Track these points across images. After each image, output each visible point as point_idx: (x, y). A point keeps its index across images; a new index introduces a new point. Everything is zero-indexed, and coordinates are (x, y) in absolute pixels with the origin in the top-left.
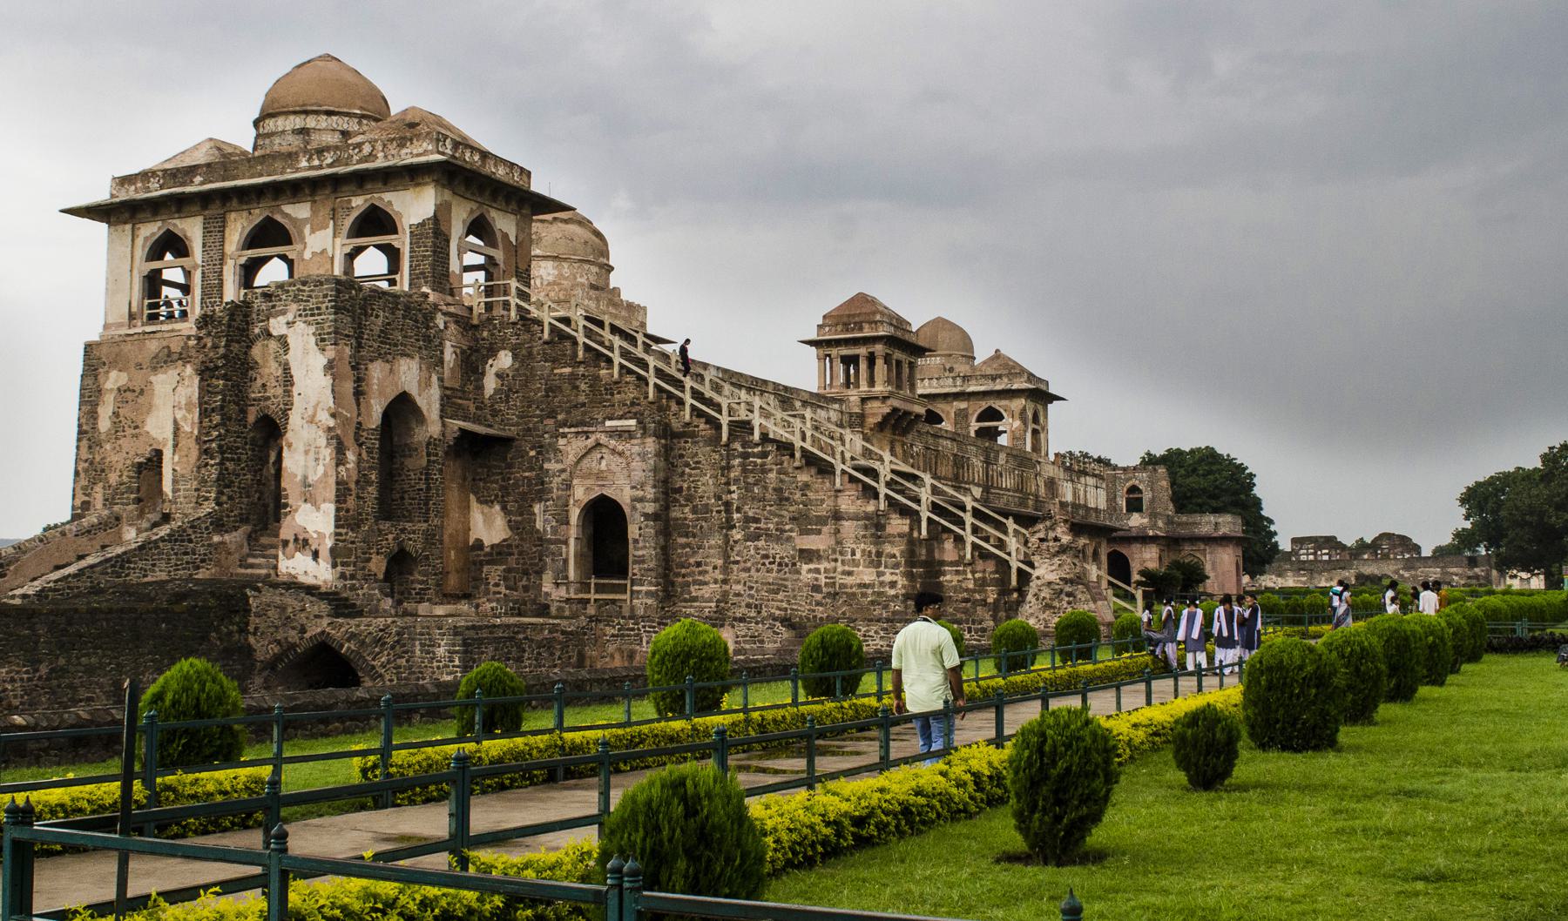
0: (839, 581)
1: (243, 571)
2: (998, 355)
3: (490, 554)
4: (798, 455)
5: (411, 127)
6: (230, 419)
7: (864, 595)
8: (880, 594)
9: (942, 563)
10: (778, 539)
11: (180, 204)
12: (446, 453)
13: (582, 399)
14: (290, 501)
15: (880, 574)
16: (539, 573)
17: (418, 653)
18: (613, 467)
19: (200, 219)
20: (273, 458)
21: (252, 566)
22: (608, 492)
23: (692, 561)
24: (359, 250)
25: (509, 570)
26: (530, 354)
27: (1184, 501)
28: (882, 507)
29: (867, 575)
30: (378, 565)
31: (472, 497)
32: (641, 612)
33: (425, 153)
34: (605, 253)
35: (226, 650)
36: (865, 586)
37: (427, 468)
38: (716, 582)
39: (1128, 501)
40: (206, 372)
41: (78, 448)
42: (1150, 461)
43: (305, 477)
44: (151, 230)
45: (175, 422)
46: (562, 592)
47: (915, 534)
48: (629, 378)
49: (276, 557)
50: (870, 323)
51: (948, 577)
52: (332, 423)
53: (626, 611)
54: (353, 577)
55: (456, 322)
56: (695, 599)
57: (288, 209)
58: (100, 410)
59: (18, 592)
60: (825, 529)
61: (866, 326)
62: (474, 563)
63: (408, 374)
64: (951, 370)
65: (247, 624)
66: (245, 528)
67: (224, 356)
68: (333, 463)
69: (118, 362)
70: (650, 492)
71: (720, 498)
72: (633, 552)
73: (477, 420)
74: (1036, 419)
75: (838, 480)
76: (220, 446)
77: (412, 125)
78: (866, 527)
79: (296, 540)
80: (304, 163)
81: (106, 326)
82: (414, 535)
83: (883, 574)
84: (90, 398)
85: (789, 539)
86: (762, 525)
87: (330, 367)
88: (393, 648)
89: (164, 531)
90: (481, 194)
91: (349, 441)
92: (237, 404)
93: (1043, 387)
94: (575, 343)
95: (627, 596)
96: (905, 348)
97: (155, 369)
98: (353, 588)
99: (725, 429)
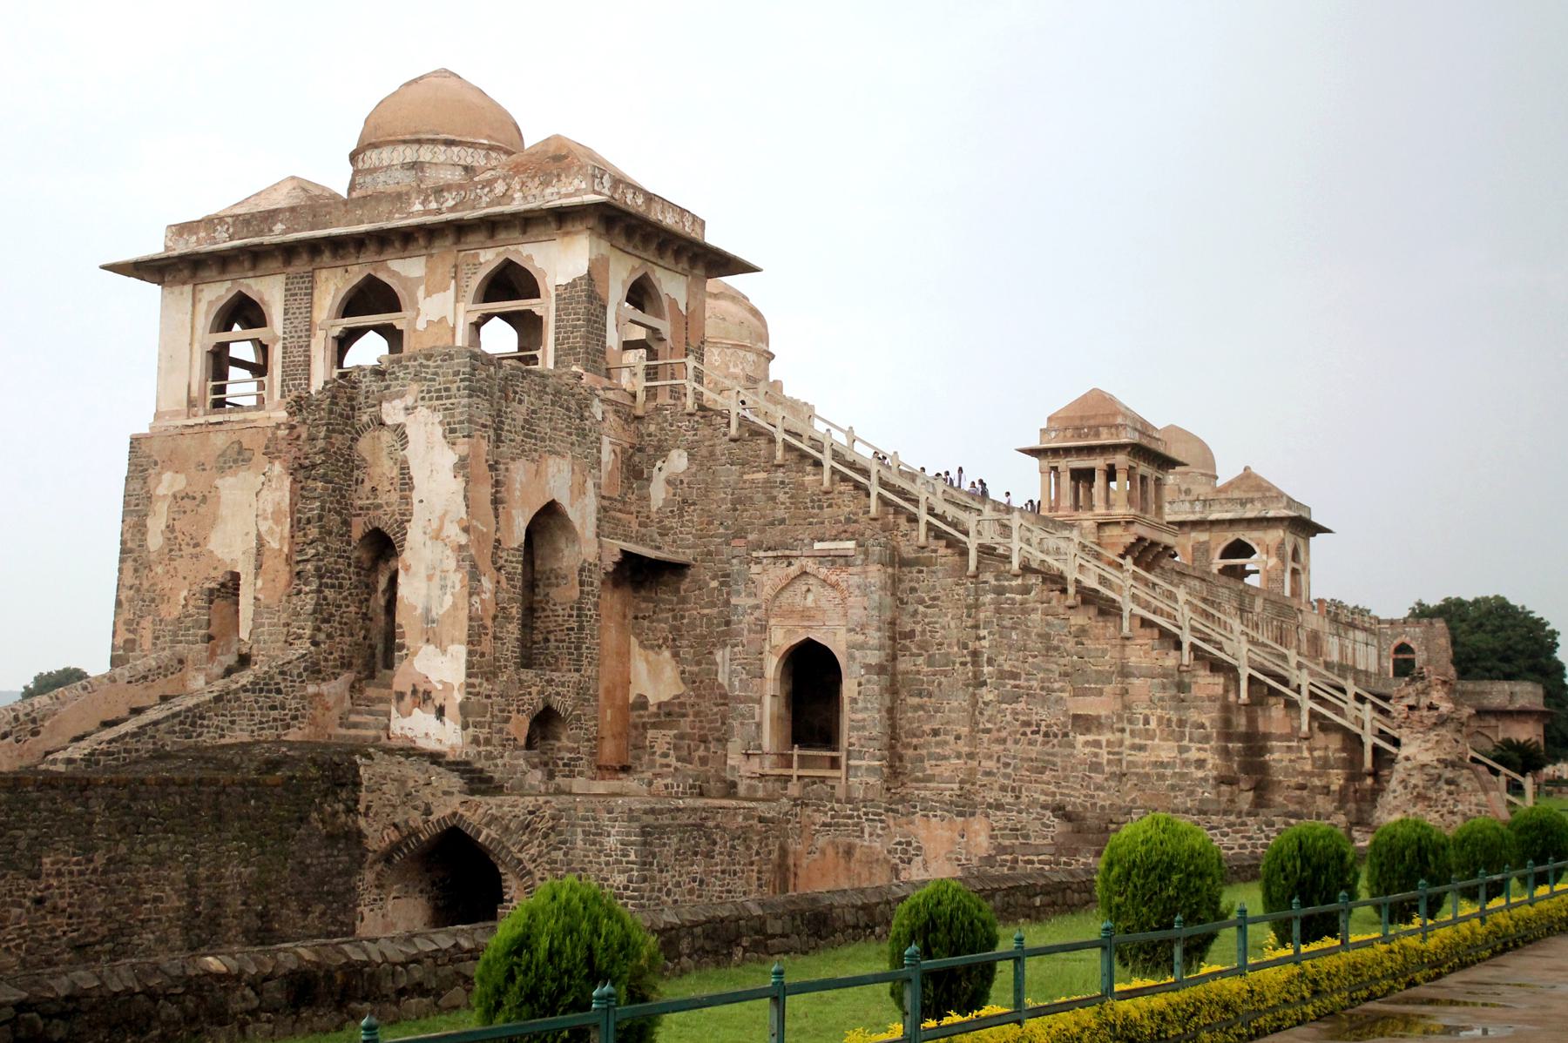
0: (1126, 758)
1: (343, 731)
2: (1247, 475)
3: (658, 715)
4: (1071, 590)
5: (559, 158)
6: (330, 533)
7: (1161, 777)
8: (1183, 776)
9: (1267, 736)
10: (1044, 700)
11: (255, 257)
12: (603, 583)
13: (781, 513)
14: (407, 641)
15: (1182, 750)
16: (723, 741)
17: (580, 843)
18: (823, 603)
19: (281, 278)
20: (383, 582)
21: (355, 726)
22: (817, 636)
23: (927, 728)
24: (487, 318)
25: (681, 737)
26: (712, 454)
27: (1468, 664)
28: (1186, 661)
29: (1165, 751)
30: (519, 726)
31: (633, 639)
32: (860, 794)
33: (577, 192)
34: (764, 338)
35: (330, 836)
36: (1162, 765)
37: (580, 602)
38: (959, 756)
39: (1396, 663)
40: (300, 471)
41: (120, 570)
42: (1422, 613)
43: (428, 610)
44: (217, 293)
45: (259, 537)
46: (754, 765)
47: (1232, 697)
48: (843, 487)
49: (388, 714)
50: (1110, 427)
51: (1276, 756)
52: (463, 539)
53: (840, 792)
54: (488, 742)
55: (617, 412)
56: (930, 778)
57: (396, 265)
58: (149, 522)
59: (61, 755)
60: (1108, 688)
61: (1104, 431)
62: (635, 727)
63: (557, 479)
64: (1188, 492)
65: (357, 802)
66: (347, 677)
67: (323, 451)
68: (466, 591)
69: (174, 461)
70: (874, 637)
71: (965, 646)
72: (847, 716)
73: (641, 540)
74: (1295, 556)
75: (1126, 624)
76: (318, 569)
77: (558, 158)
78: (1164, 687)
79: (415, 692)
80: (418, 207)
81: (158, 415)
83: (1187, 749)
84: (136, 507)
85: (1059, 701)
86: (1022, 683)
87: (462, 466)
88: (546, 836)
89: (245, 677)
90: (645, 247)
91: (485, 564)
92: (339, 513)
93: (1305, 515)
94: (772, 441)
95: (841, 773)
96: (1152, 457)
97: (221, 470)
98: (489, 756)
99: (973, 555)
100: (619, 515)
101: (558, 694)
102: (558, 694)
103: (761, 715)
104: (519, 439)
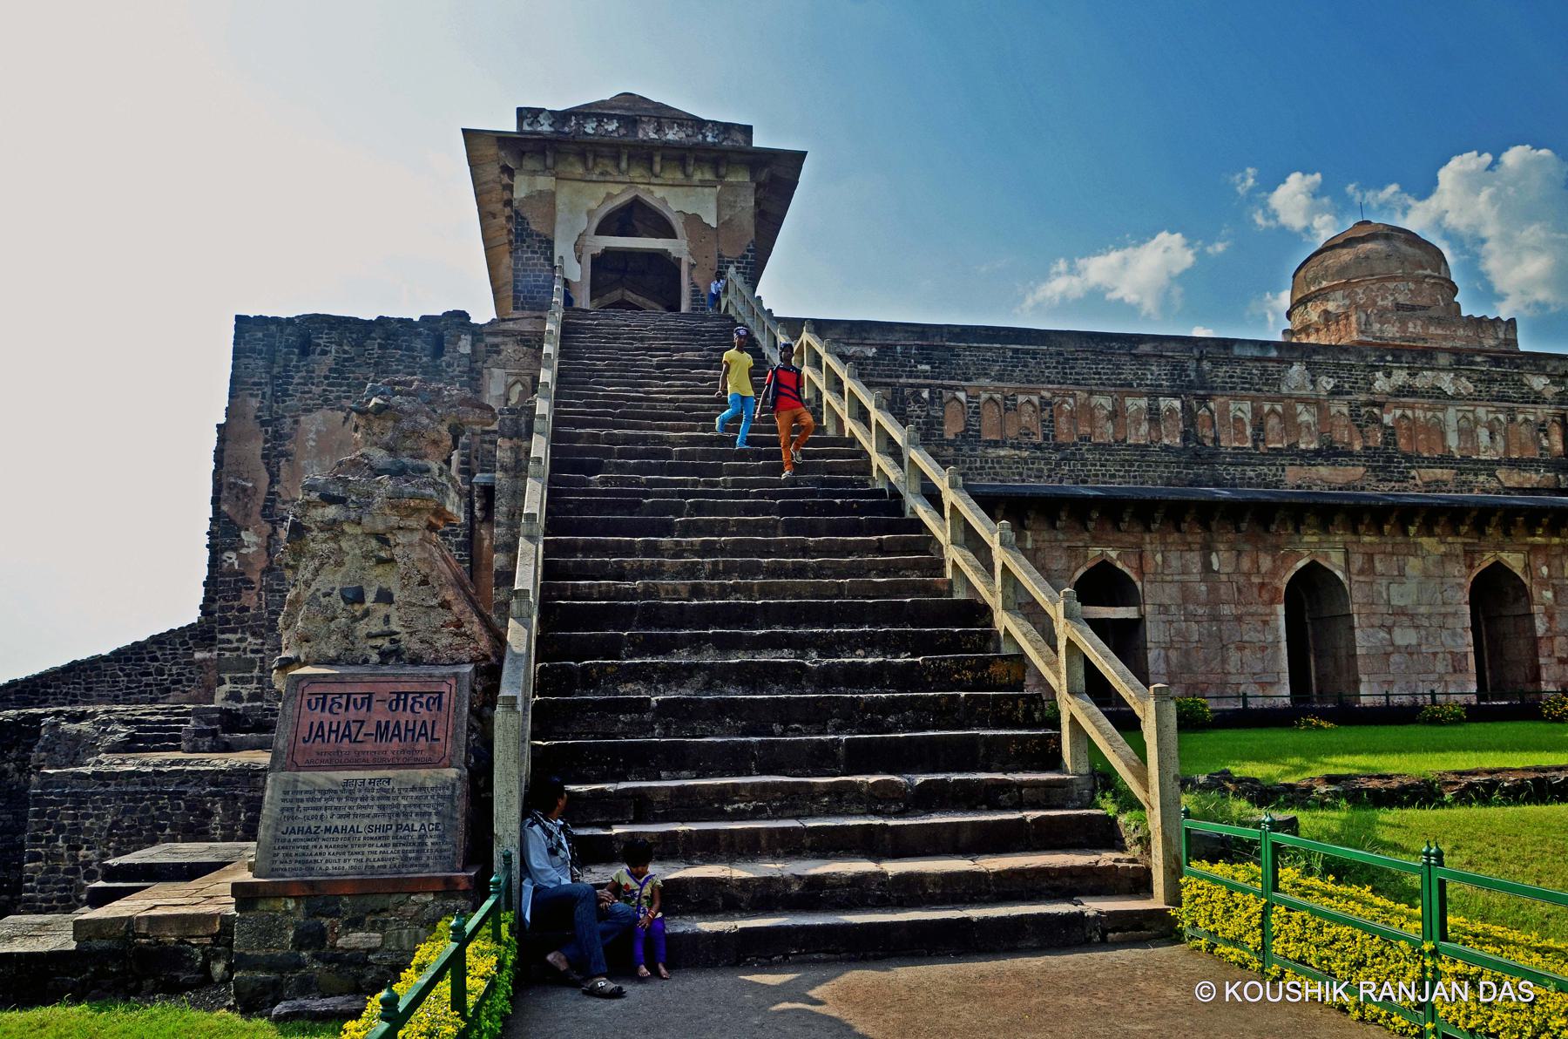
104: (316, 390)
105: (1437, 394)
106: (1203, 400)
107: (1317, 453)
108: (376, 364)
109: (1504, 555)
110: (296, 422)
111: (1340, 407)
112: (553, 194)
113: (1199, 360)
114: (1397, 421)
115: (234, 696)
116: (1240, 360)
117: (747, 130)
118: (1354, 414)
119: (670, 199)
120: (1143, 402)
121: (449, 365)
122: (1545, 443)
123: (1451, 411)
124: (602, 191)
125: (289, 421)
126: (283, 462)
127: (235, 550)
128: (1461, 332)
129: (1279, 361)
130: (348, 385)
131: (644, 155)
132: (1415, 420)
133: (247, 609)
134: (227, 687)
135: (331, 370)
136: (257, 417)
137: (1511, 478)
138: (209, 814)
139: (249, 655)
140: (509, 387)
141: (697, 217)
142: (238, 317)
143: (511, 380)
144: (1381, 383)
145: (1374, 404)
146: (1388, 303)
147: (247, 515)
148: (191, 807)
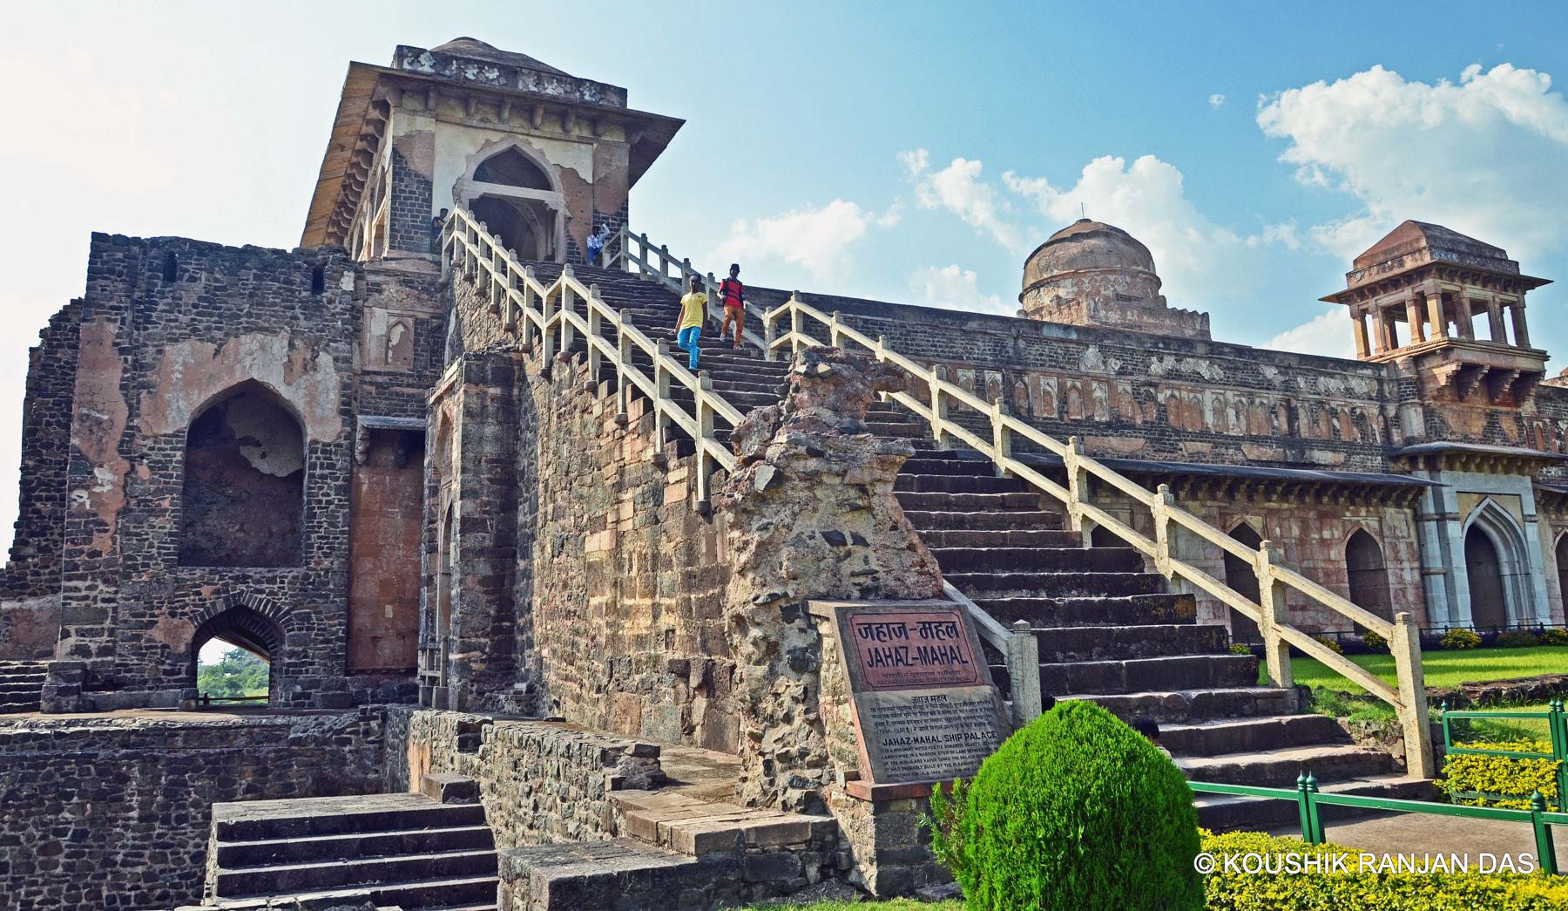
63: (261, 359)
82: (269, 590)
100: (406, 390)
101: (262, 592)
102: (262, 592)
103: (432, 601)
105: (1197, 378)
106: (1020, 374)
107: (1109, 425)
108: (251, 295)
109: (1248, 517)
110: (160, 352)
111: (1124, 386)
112: (433, 135)
113: (1016, 339)
114: (1168, 399)
115: (81, 650)
116: (1048, 340)
117: (622, 93)
118: (1136, 393)
119: (551, 152)
120: (971, 374)
121: (331, 301)
122: (1276, 423)
123: (1208, 392)
124: (482, 137)
125: (151, 350)
126: (144, 393)
127: (87, 488)
128: (1167, 322)
129: (1078, 343)
130: (220, 316)
131: (528, 107)
132: (1181, 400)
133: (99, 554)
134: (73, 640)
135: (200, 298)
136: (115, 344)
137: (1253, 452)
138: (125, 779)
139: (100, 605)
140: (391, 328)
141: (573, 172)
142: (95, 236)
143: (393, 320)
144: (1156, 367)
145: (1151, 384)
146: (1110, 293)
147: (101, 451)
148: (102, 773)
